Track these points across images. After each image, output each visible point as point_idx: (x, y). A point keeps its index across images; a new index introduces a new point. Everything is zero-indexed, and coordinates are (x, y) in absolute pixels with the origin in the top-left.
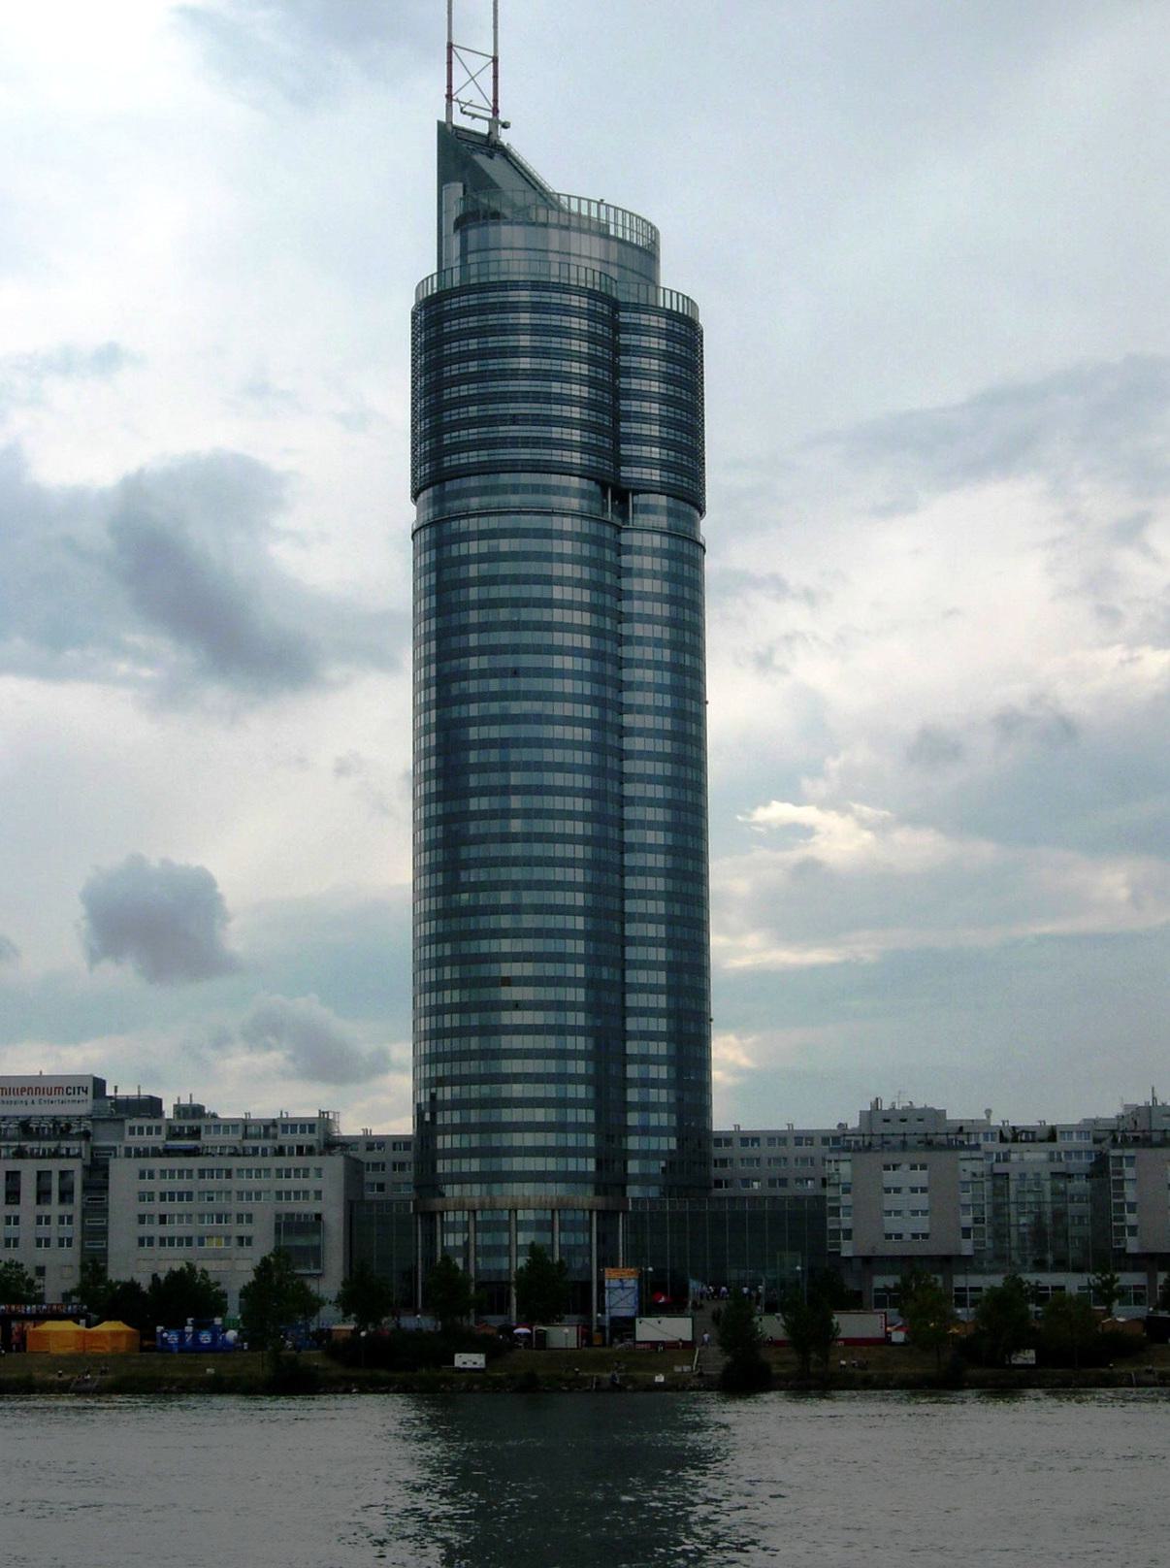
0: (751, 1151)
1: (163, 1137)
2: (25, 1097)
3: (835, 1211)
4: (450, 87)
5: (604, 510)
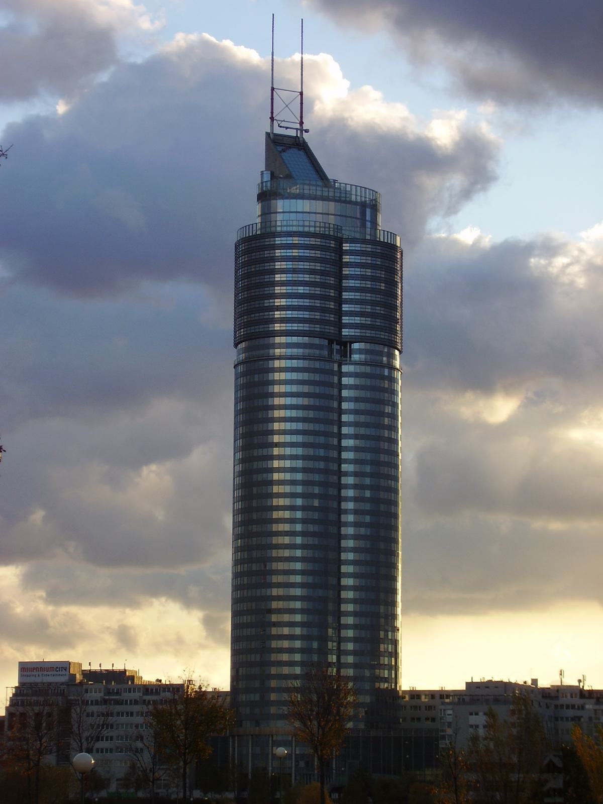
0: (415, 702)
1: (102, 694)
2: (35, 673)
3: (443, 737)
4: (272, 113)
5: (331, 351)
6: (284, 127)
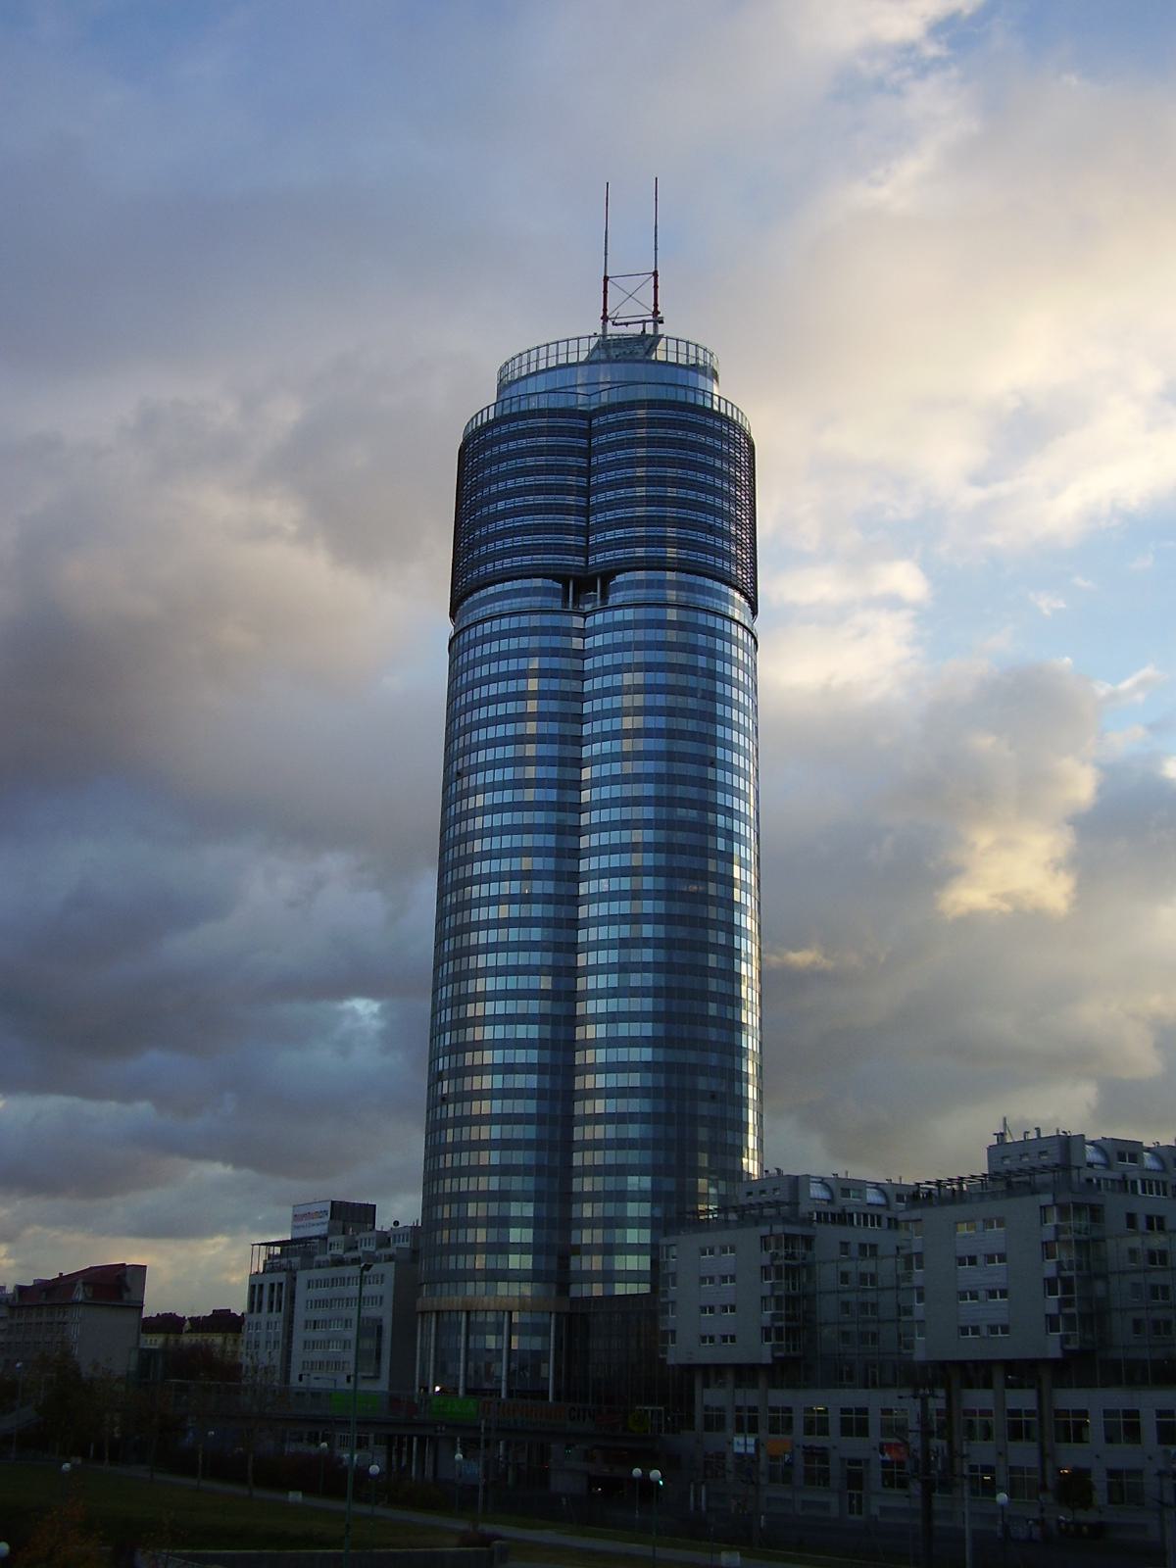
4: (605, 310)
6: (621, 324)
